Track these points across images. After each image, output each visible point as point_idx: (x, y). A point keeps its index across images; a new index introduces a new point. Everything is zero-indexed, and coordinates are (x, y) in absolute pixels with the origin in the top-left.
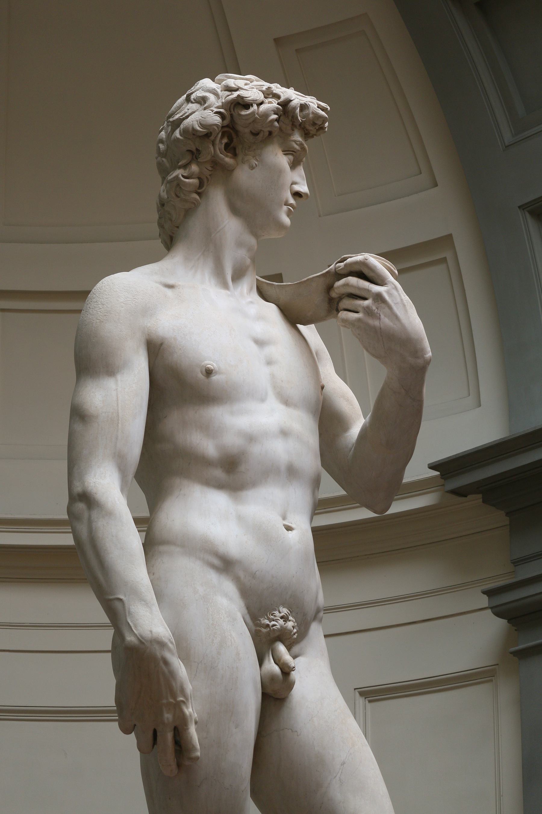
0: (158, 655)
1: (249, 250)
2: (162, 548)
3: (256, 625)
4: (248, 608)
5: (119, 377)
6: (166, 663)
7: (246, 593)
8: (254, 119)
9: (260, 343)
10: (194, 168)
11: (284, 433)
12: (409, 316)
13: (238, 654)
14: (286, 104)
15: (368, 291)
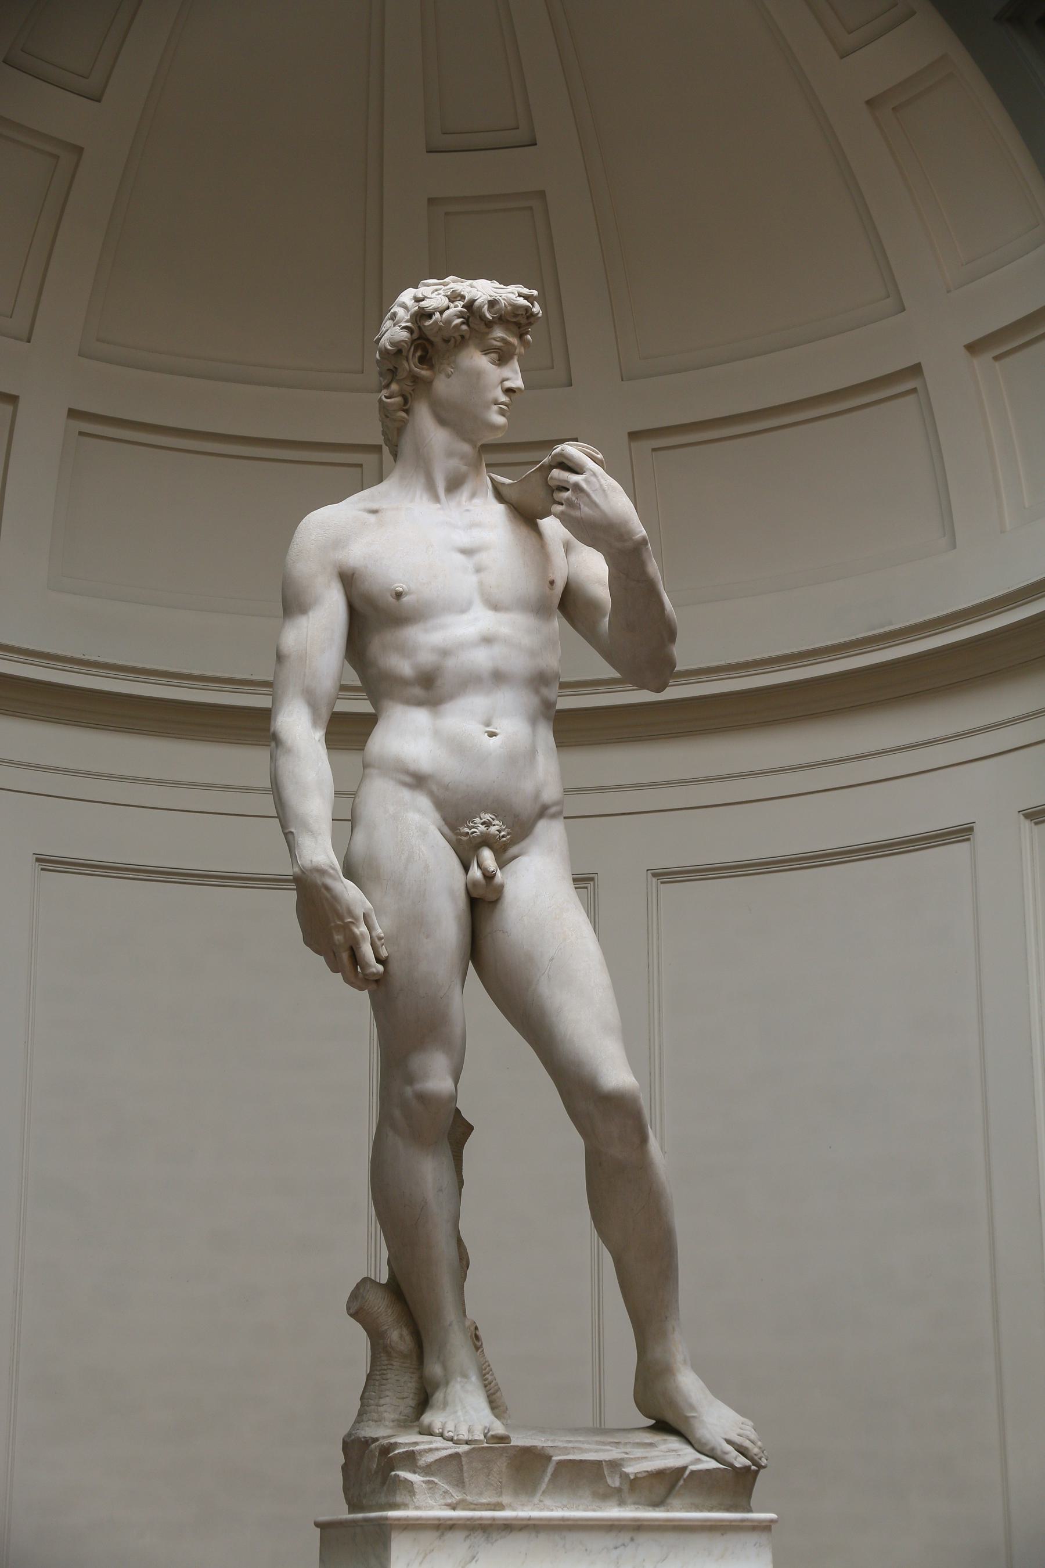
0: (319, 882)
1: (463, 457)
2: (367, 771)
3: (457, 834)
4: (444, 819)
5: (311, 614)
6: (328, 888)
7: (440, 804)
8: (438, 328)
9: (467, 552)
10: (394, 387)
11: (487, 640)
12: (615, 500)
13: (427, 867)
14: (470, 305)
15: (567, 482)
